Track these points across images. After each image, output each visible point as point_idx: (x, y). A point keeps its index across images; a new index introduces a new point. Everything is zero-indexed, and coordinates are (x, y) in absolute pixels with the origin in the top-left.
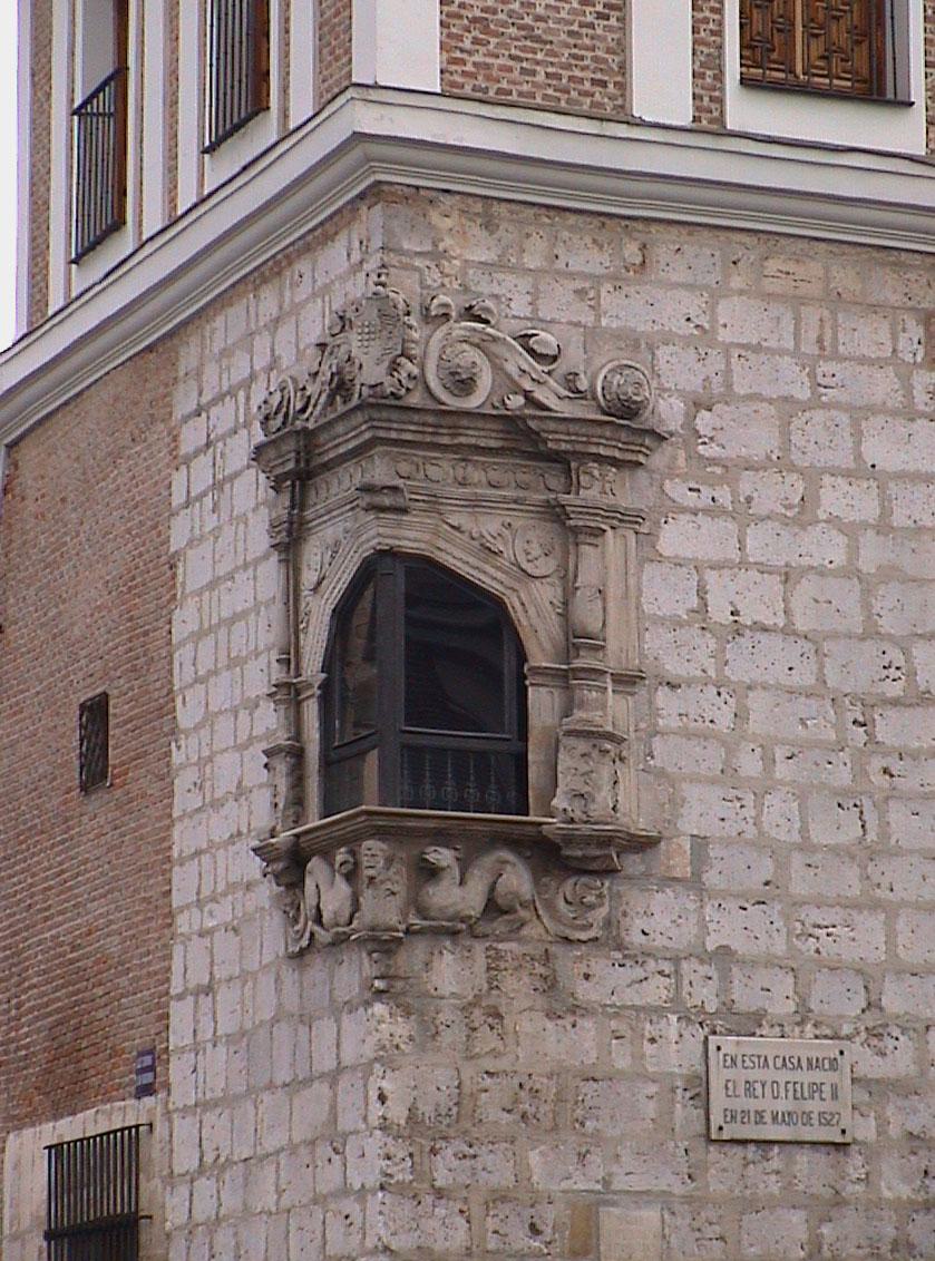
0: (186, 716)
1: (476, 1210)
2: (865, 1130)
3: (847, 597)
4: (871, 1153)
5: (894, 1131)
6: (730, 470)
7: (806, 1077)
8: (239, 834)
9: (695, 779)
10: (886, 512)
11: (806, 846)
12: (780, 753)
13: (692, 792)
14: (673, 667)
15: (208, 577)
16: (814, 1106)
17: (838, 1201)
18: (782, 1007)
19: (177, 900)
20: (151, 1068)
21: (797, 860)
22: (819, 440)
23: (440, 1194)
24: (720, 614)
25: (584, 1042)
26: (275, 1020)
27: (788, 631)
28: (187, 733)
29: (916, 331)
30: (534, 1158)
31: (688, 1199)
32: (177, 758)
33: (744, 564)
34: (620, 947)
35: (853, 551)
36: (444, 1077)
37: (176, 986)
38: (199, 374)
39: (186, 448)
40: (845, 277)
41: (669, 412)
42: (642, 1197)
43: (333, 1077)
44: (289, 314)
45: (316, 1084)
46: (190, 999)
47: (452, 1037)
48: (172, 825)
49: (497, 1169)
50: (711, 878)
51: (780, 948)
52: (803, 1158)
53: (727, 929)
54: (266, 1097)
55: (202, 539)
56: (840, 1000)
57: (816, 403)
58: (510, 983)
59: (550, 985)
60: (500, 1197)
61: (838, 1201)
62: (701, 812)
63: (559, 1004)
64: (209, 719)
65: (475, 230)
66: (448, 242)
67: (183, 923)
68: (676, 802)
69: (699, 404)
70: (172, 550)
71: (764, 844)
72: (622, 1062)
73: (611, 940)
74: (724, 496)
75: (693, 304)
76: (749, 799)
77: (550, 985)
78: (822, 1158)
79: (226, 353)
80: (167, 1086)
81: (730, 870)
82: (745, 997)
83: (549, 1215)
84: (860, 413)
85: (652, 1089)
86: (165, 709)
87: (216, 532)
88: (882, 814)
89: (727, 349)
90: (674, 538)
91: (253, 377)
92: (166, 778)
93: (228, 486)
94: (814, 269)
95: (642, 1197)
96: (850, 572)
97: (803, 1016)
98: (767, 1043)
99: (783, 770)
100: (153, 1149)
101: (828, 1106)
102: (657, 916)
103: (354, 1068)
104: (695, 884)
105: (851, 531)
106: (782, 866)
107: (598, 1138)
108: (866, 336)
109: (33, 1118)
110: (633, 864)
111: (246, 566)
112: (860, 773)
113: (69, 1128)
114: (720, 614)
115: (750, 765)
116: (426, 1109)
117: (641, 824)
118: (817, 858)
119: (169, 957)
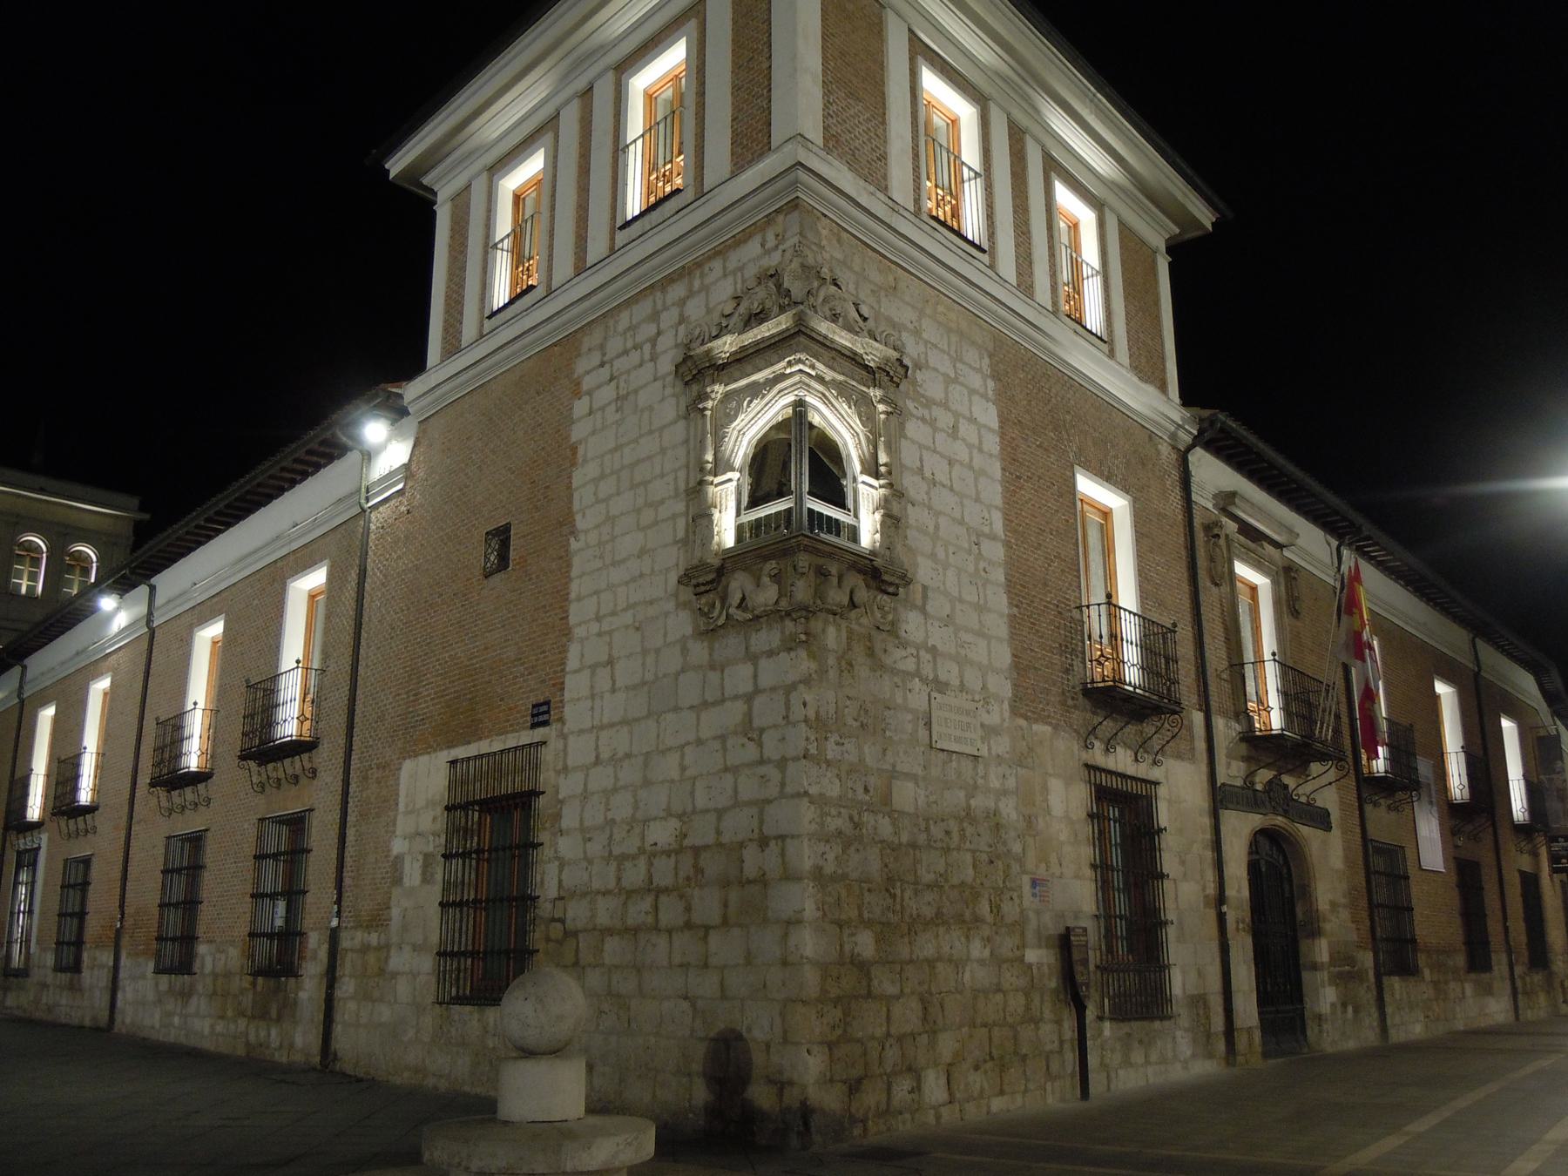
0: (580, 523)
1: (843, 775)
2: (984, 752)
6: (929, 403)
8: (641, 575)
11: (961, 601)
14: (912, 493)
15: (612, 445)
16: (968, 734)
19: (572, 620)
20: (548, 712)
23: (828, 763)
24: (928, 474)
26: (683, 671)
27: (951, 489)
28: (586, 532)
29: (986, 360)
30: (866, 749)
32: (574, 545)
33: (935, 451)
34: (898, 637)
36: (830, 696)
37: (572, 662)
38: (602, 347)
39: (585, 387)
43: (749, 698)
44: (699, 292)
45: (728, 704)
46: (587, 672)
47: (832, 674)
48: (571, 580)
51: (953, 651)
54: (670, 716)
55: (604, 428)
59: (871, 652)
64: (611, 519)
66: (824, 243)
67: (579, 632)
69: (918, 366)
70: (573, 439)
72: (899, 701)
74: (926, 413)
77: (871, 652)
79: (632, 328)
80: (561, 720)
83: (873, 781)
84: (972, 392)
85: (910, 717)
86: (565, 524)
87: (618, 423)
89: (926, 342)
91: (659, 333)
92: (565, 559)
93: (632, 398)
94: (952, 316)
100: (548, 755)
103: (773, 689)
105: (970, 446)
109: (429, 749)
111: (651, 432)
113: (461, 752)
116: (823, 713)
119: (566, 651)
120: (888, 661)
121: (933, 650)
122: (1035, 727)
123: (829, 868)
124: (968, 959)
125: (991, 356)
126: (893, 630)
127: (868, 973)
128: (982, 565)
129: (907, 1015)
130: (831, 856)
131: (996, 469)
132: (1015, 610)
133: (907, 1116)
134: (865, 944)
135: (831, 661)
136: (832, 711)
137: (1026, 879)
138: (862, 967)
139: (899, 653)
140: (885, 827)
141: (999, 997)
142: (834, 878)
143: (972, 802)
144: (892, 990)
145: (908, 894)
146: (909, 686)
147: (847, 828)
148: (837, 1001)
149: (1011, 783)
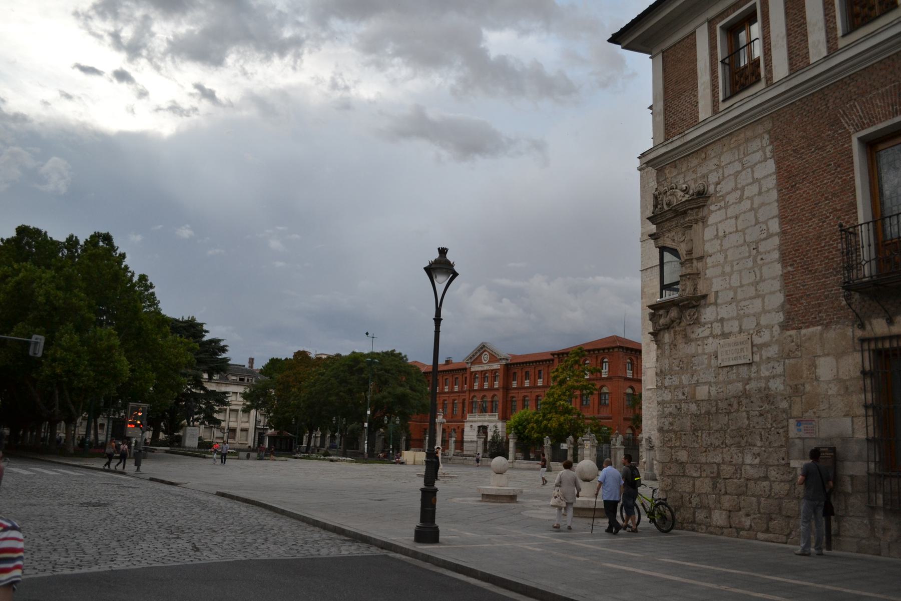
2: (757, 358)
3: (751, 216)
4: (758, 364)
5: (764, 357)
7: (739, 347)
9: (716, 277)
10: (760, 189)
12: (735, 263)
13: (714, 280)
16: (743, 354)
17: (750, 379)
18: (736, 329)
21: (739, 290)
22: (745, 178)
23: (666, 388)
24: (721, 234)
25: (691, 349)
31: (715, 383)
35: (752, 204)
36: (667, 361)
40: (749, 133)
41: (711, 189)
42: (705, 383)
47: (667, 352)
49: (676, 381)
50: (719, 301)
52: (741, 369)
53: (724, 312)
56: (749, 324)
57: (743, 169)
58: (678, 337)
60: (676, 387)
61: (750, 379)
62: (717, 285)
63: (687, 340)
65: (673, 169)
68: (711, 284)
69: (718, 183)
71: (731, 288)
73: (697, 322)
74: (722, 204)
75: (715, 161)
76: (727, 278)
77: (685, 336)
78: (746, 368)
81: (725, 297)
82: (727, 330)
83: (686, 390)
88: (761, 270)
90: (712, 220)
94: (742, 135)
95: (705, 383)
96: (752, 209)
97: (741, 331)
98: (732, 339)
99: (736, 268)
101: (746, 354)
102: (708, 314)
104: (715, 304)
106: (735, 293)
107: (696, 371)
108: (755, 145)
110: (703, 302)
112: (755, 261)
114: (721, 234)
115: (728, 269)
117: (704, 292)
118: (744, 288)
120: (693, 336)
121: (722, 320)
122: (803, 331)
123: (666, 428)
124: (743, 463)
125: (769, 132)
126: (697, 322)
127: (684, 467)
128: (759, 257)
129: (704, 486)
130: (667, 423)
131: (774, 195)
132: (790, 269)
133: (704, 527)
134: (683, 456)
135: (667, 347)
136: (667, 367)
137: (792, 422)
138: (682, 464)
139: (700, 330)
140: (693, 407)
141: (766, 483)
142: (668, 431)
143: (747, 387)
144: (695, 475)
145: (704, 436)
146: (706, 342)
147: (674, 411)
148: (669, 476)
149: (779, 370)
